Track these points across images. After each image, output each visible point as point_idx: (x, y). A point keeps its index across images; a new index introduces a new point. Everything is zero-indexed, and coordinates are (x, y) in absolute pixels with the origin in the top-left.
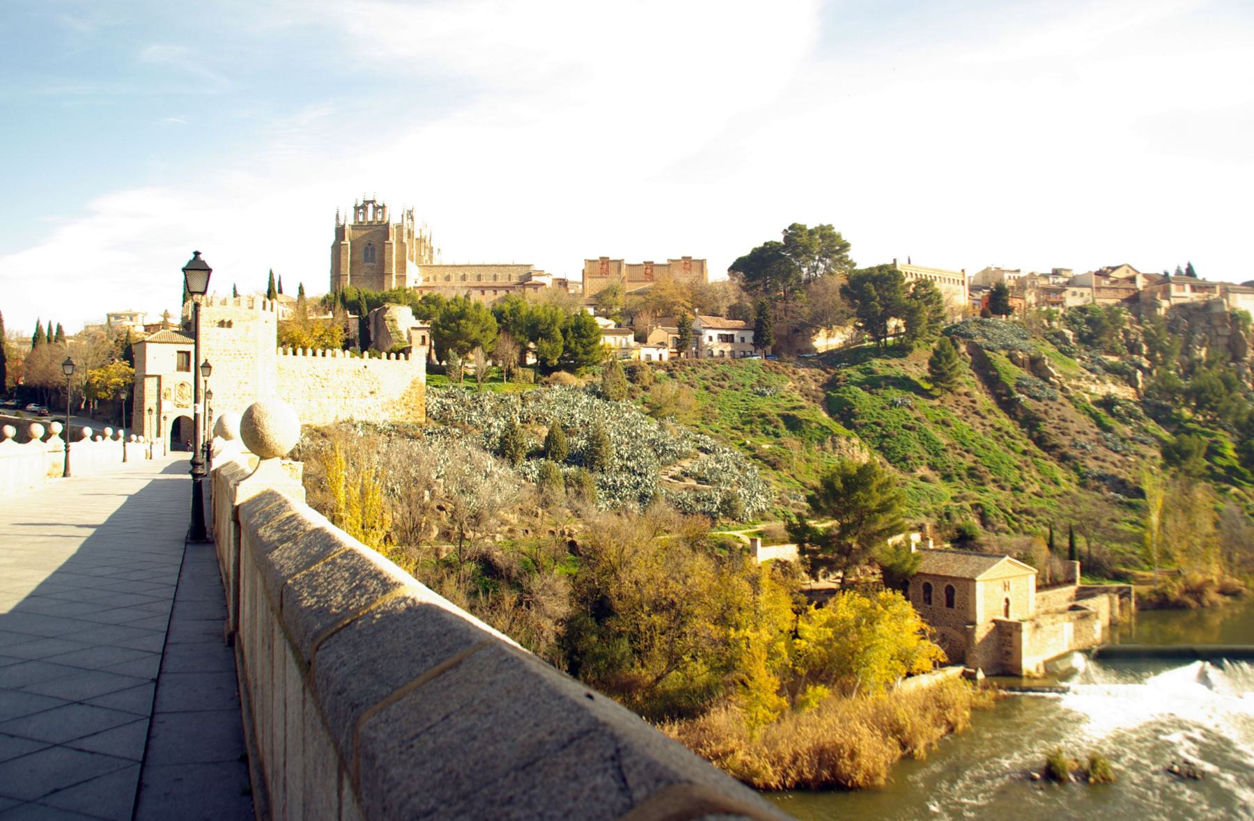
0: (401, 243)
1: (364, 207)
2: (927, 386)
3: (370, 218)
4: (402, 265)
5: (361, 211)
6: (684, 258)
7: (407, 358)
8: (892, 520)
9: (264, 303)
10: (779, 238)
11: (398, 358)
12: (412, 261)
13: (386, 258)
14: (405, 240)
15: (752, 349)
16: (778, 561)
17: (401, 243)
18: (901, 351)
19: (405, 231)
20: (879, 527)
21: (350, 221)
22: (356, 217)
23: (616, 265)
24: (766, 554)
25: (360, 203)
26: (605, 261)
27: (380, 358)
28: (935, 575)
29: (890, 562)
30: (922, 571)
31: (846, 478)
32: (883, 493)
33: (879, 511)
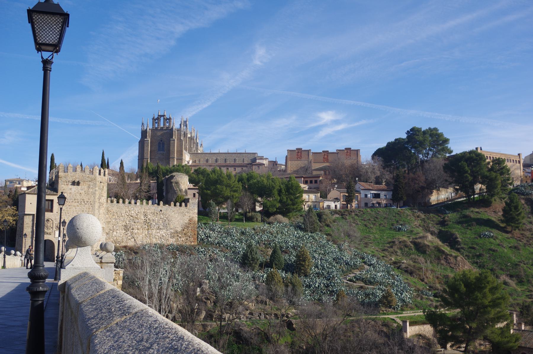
0: (180, 140)
1: (158, 119)
2: (503, 225)
3: (162, 126)
4: (180, 154)
5: (157, 121)
6: (346, 149)
7: (186, 206)
8: (500, 312)
9: (100, 171)
10: (428, 128)
11: (181, 206)
12: (186, 150)
13: (171, 149)
14: (182, 138)
15: (391, 202)
16: (420, 335)
17: (180, 140)
18: (484, 202)
19: (182, 133)
20: (491, 316)
21: (150, 127)
22: (153, 125)
23: (307, 152)
24: (411, 331)
25: (156, 117)
26: (299, 150)
27: (170, 205)
28: (529, 348)
29: (497, 340)
30: (523, 345)
31: (467, 284)
32: (493, 294)
33: (490, 306)
